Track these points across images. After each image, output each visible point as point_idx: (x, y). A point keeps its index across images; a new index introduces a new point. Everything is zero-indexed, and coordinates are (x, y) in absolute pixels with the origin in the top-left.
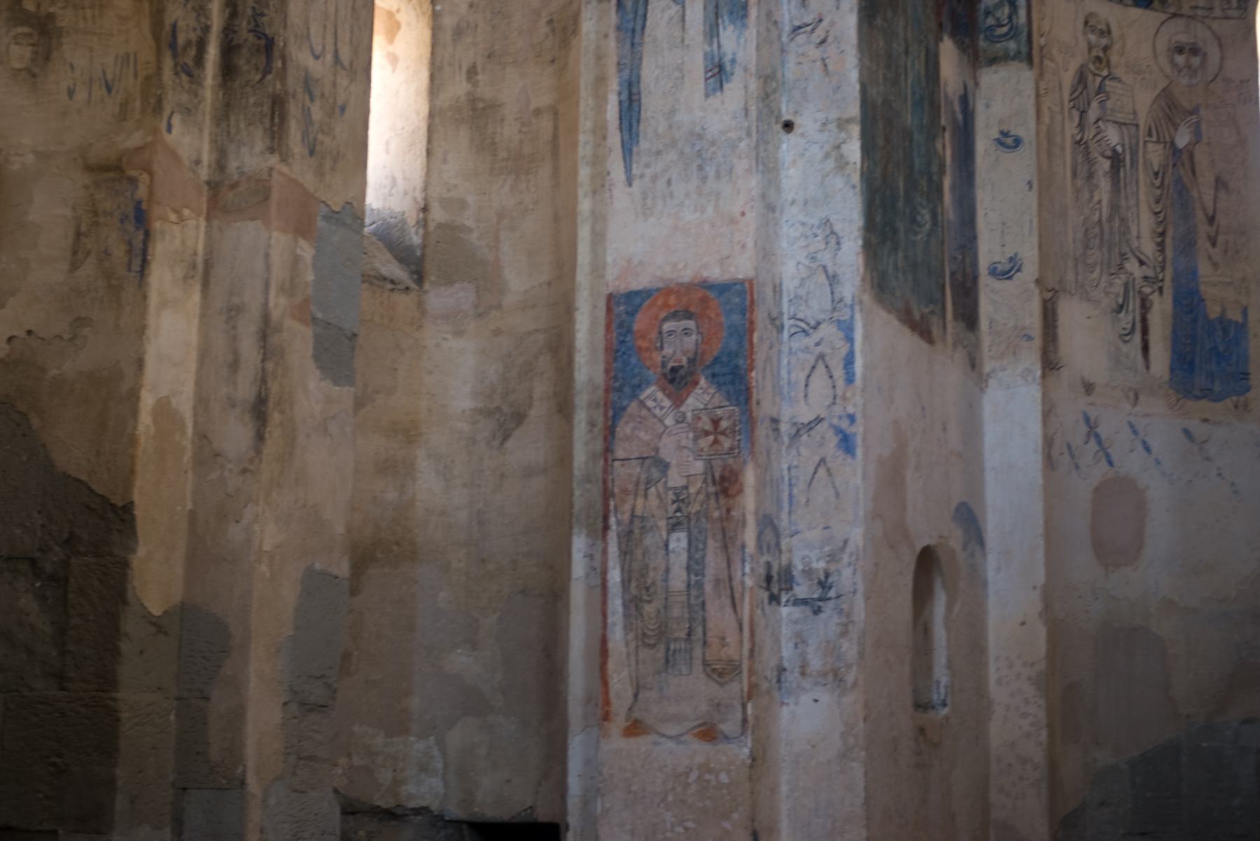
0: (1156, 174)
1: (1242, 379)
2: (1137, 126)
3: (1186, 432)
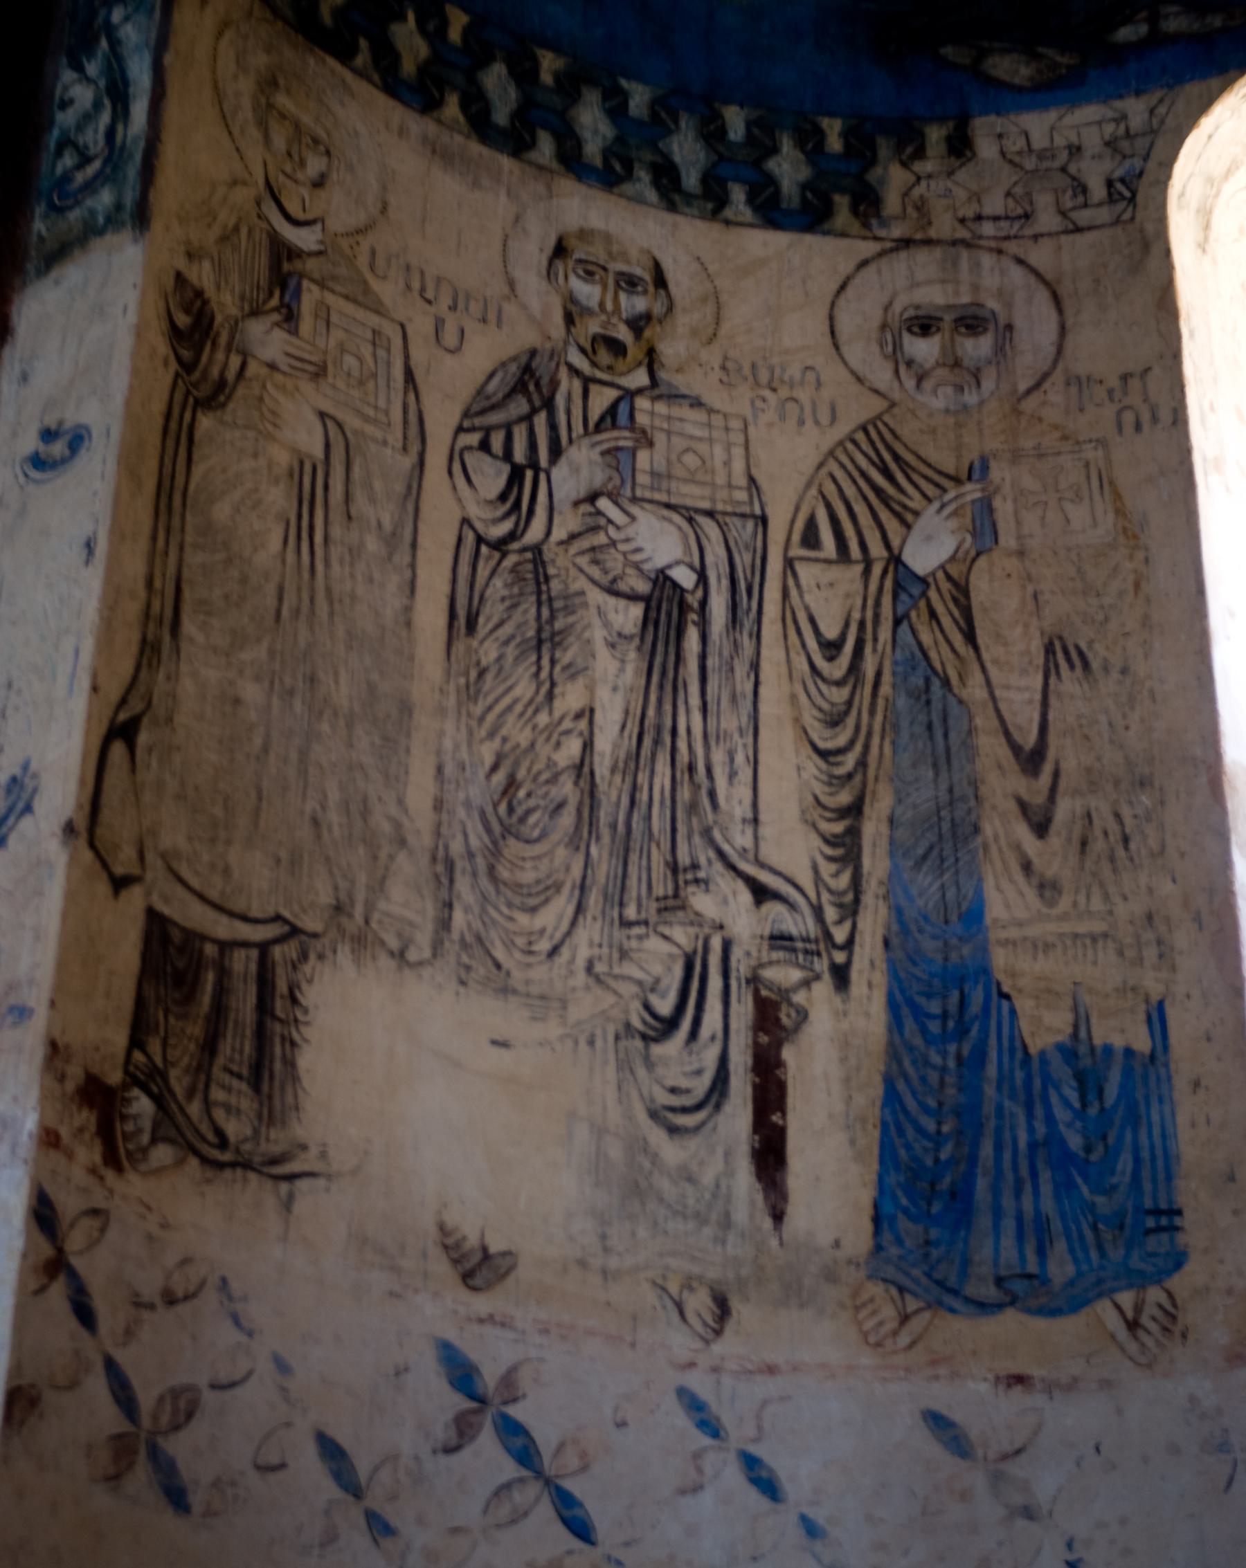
0: (832, 648)
1: (1159, 1229)
2: (763, 520)
3: (937, 1421)
